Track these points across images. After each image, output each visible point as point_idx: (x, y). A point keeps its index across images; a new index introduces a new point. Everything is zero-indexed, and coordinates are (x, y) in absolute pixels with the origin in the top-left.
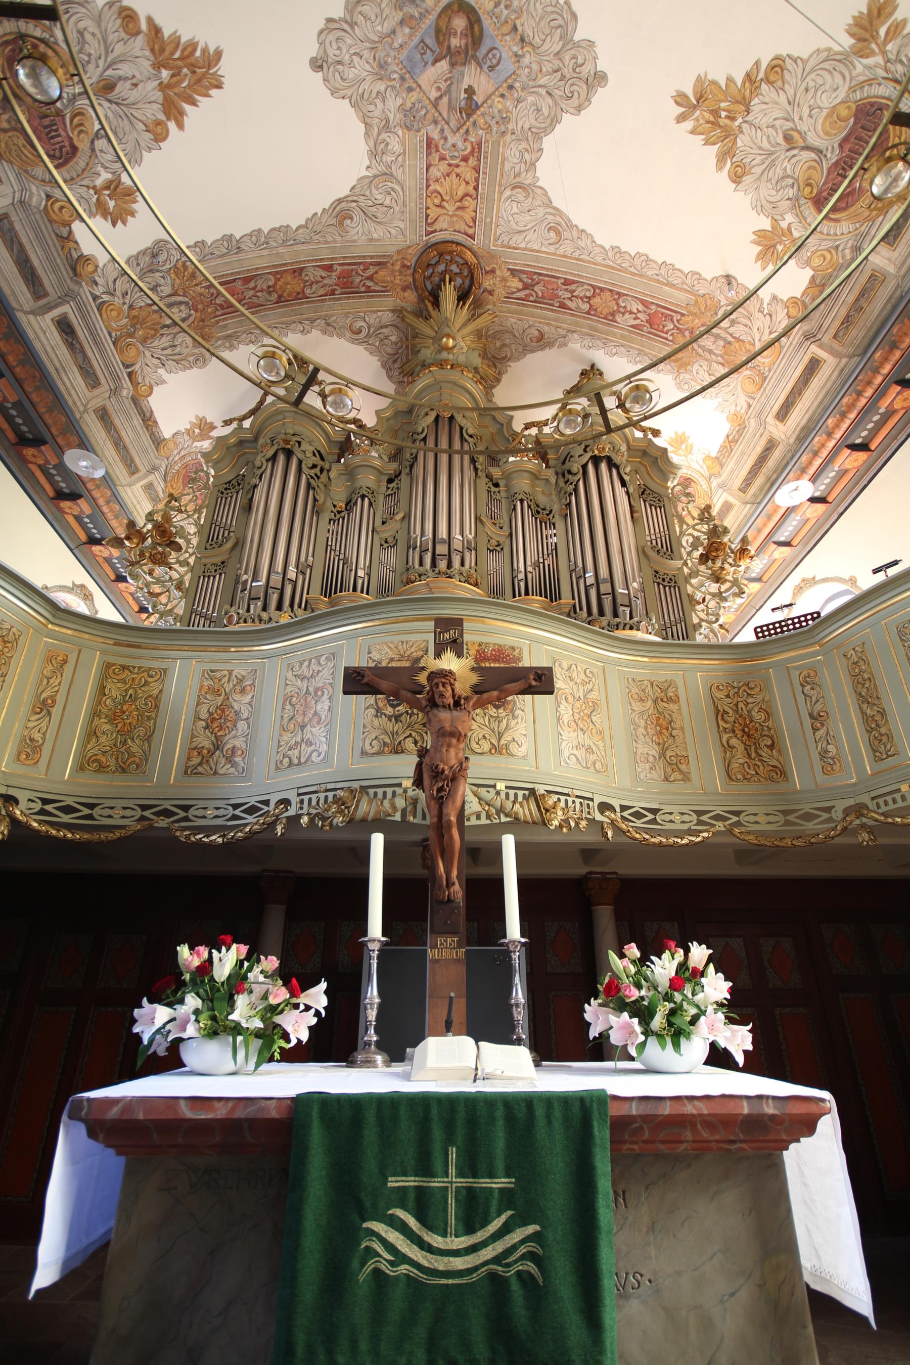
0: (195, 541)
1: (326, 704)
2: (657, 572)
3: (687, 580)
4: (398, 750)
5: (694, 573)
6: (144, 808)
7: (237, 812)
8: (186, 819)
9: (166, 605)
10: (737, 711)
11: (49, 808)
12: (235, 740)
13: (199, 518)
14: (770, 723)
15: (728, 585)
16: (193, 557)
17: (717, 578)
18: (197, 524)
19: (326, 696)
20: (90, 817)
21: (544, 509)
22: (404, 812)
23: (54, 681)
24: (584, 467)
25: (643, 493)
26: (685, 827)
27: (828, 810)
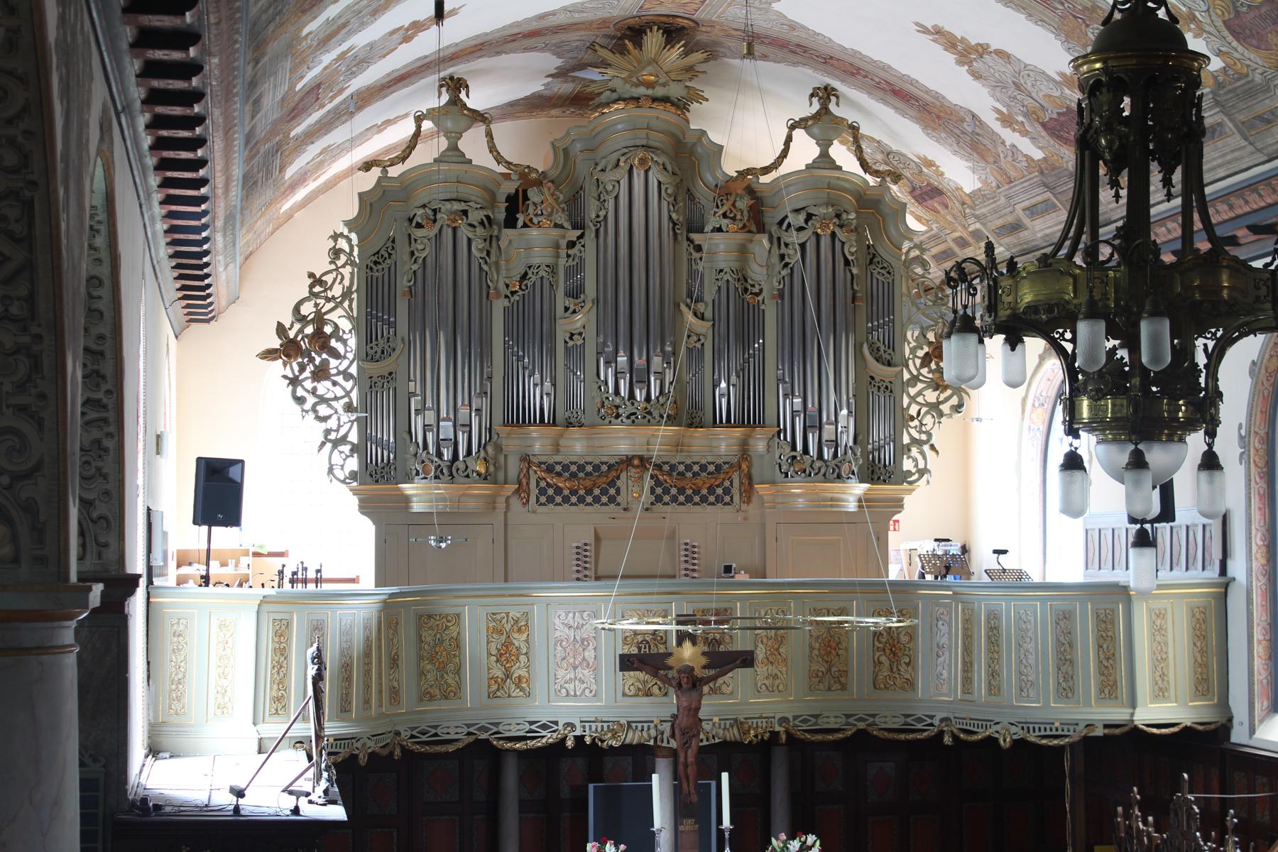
0: (352, 342)
1: (592, 654)
2: (872, 378)
3: (905, 385)
4: (648, 694)
5: (915, 379)
6: (469, 726)
7: (533, 727)
8: (498, 733)
9: (337, 431)
10: (889, 634)
11: (414, 733)
12: (518, 672)
13: (350, 306)
14: (911, 646)
15: (949, 392)
16: (355, 365)
17: (938, 385)
18: (350, 318)
19: (591, 647)
20: (436, 735)
21: (753, 286)
22: (656, 739)
23: (395, 641)
24: (803, 246)
25: (871, 263)
26: (836, 726)
27: (932, 717)
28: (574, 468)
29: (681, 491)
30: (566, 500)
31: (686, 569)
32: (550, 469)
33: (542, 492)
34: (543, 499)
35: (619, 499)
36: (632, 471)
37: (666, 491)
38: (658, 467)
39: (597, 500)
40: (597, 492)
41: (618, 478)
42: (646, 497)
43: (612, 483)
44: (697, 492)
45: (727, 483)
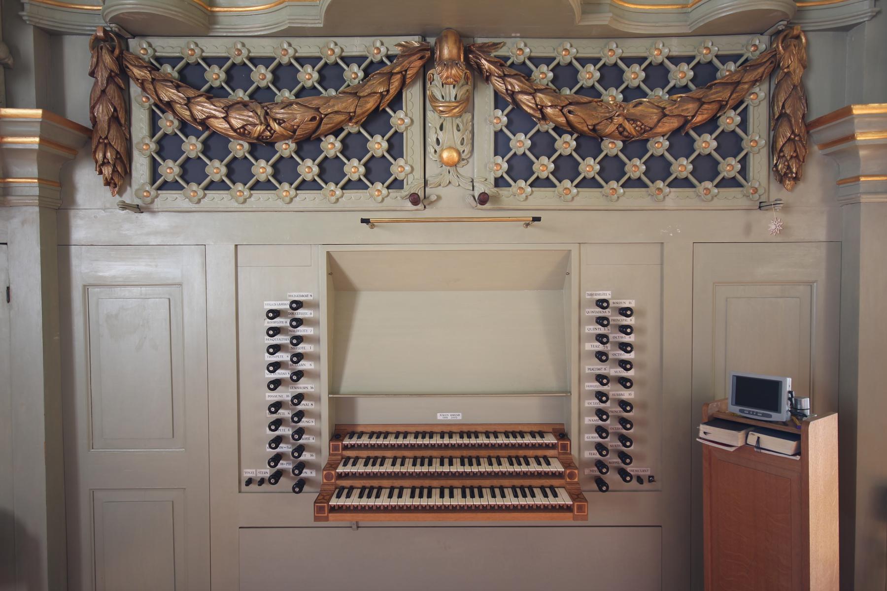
28: (262, 76)
29: (590, 142)
30: (238, 172)
31: (601, 378)
32: (190, 76)
33: (166, 147)
34: (170, 170)
35: (398, 168)
36: (444, 85)
37: (543, 145)
38: (523, 71)
39: (330, 171)
40: (331, 146)
41: (397, 102)
42: (486, 165)
43: (376, 120)
44: (635, 145)
45: (730, 120)
